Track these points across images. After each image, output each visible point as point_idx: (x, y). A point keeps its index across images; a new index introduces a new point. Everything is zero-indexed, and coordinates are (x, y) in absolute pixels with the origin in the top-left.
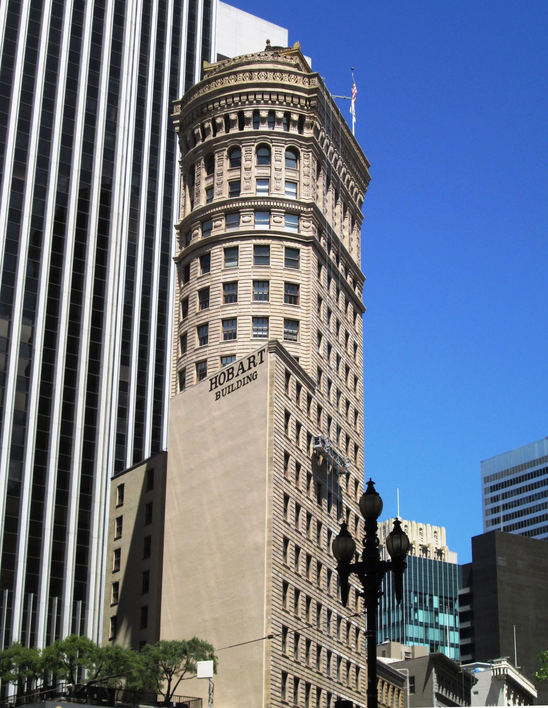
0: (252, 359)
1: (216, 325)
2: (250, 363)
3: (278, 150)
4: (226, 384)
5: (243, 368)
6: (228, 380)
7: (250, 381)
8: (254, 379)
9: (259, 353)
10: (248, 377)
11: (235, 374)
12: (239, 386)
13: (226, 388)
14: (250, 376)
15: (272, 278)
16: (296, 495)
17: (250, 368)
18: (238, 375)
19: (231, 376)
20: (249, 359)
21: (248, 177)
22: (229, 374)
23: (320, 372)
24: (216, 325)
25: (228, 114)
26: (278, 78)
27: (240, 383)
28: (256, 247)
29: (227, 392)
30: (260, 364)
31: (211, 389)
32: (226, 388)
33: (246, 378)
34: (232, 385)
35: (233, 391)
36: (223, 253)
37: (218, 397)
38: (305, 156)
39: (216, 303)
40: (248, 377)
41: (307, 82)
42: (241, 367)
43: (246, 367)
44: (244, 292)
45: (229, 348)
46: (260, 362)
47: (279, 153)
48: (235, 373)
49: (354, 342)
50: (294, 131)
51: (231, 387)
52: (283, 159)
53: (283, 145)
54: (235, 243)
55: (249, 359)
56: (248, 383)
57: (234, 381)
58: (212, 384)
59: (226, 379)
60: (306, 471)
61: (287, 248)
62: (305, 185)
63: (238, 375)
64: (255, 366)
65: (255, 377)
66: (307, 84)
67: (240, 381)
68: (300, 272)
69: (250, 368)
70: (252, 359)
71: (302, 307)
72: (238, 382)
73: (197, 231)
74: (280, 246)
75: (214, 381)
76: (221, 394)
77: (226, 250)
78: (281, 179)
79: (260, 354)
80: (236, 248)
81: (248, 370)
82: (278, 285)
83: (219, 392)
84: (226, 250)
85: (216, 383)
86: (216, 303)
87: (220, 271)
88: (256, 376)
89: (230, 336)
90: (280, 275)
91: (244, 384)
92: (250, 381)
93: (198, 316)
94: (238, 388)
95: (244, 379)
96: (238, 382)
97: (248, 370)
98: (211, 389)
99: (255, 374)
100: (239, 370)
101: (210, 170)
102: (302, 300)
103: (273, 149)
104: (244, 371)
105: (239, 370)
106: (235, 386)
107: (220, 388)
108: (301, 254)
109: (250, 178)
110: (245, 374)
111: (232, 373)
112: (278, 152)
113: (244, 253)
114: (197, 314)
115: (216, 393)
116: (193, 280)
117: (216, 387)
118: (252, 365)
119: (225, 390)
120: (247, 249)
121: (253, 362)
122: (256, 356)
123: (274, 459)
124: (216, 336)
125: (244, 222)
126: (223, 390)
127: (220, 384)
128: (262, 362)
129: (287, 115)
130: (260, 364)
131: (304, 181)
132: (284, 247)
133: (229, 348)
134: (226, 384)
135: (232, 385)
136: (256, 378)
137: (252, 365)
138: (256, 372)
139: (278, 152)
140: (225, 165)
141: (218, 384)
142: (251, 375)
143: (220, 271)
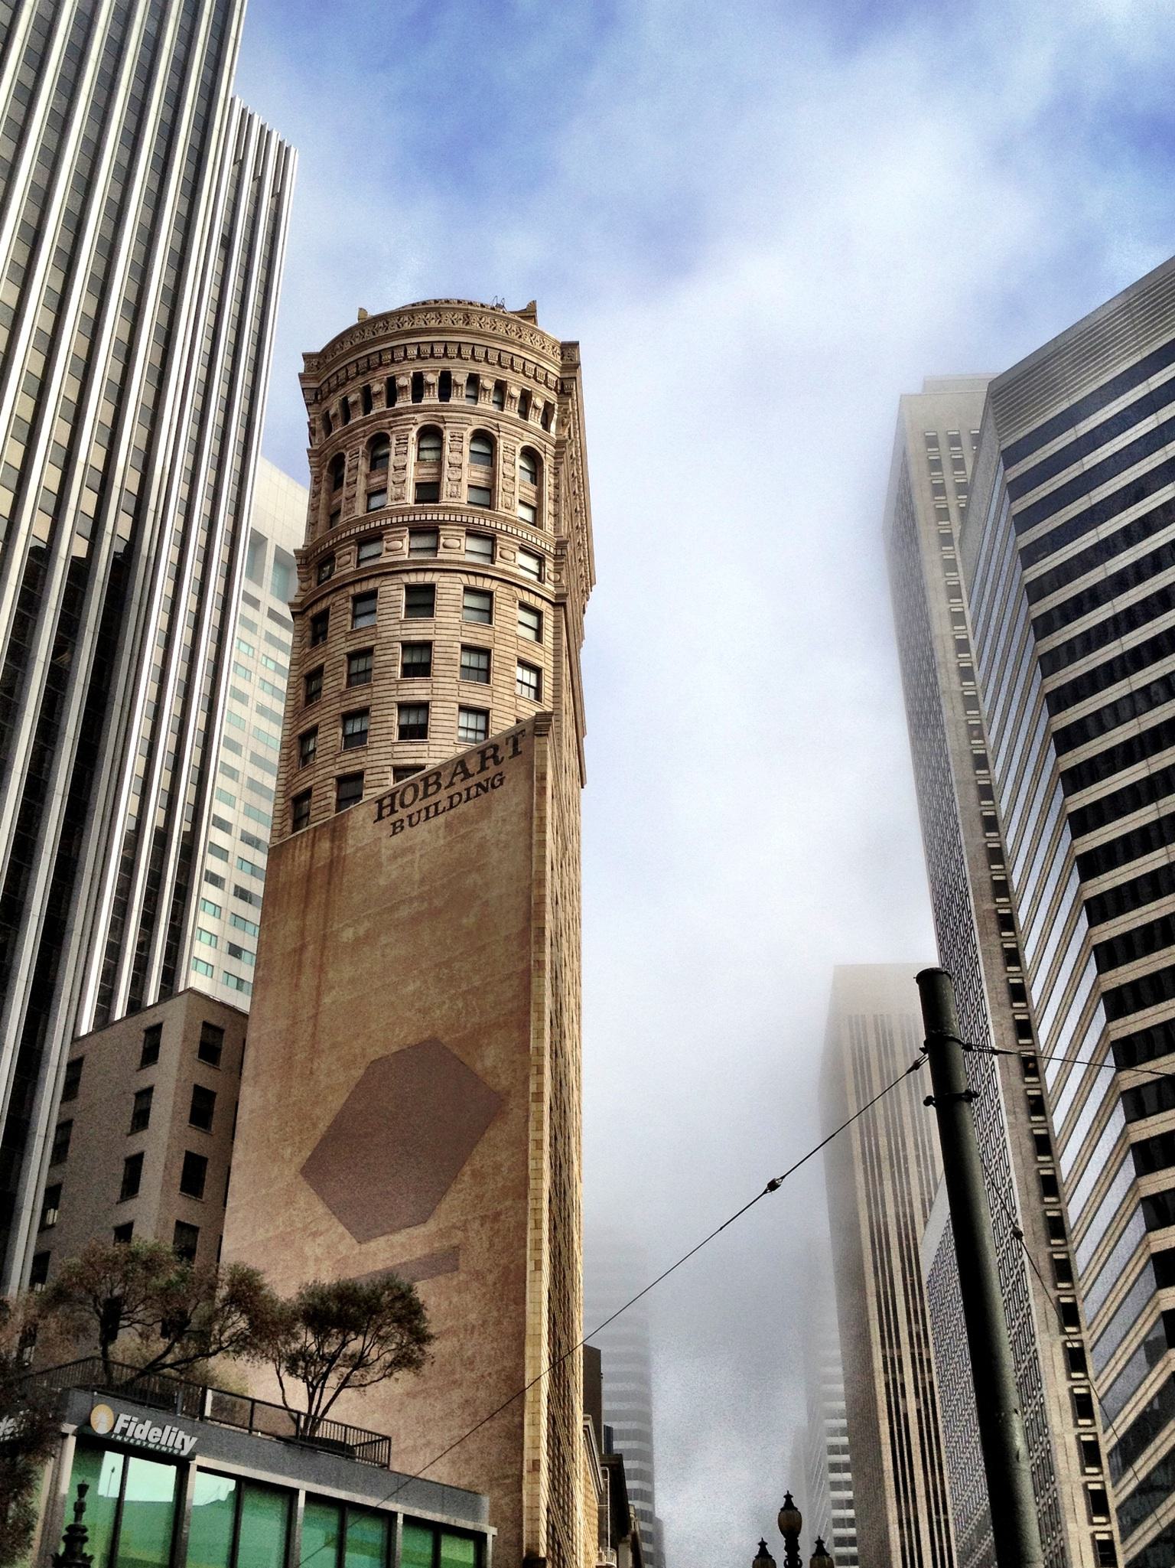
0: (490, 752)
1: (386, 712)
2: (484, 759)
4: (420, 805)
5: (465, 771)
6: (426, 795)
8: (493, 787)
13: (419, 812)
14: (485, 784)
15: (496, 646)
17: (483, 768)
18: (451, 784)
19: (431, 790)
21: (456, 477)
22: (427, 786)
24: (386, 712)
25: (421, 373)
27: (456, 799)
29: (422, 819)
30: (510, 758)
31: (380, 817)
32: (419, 812)
34: (436, 804)
35: (437, 814)
36: (403, 592)
37: (397, 828)
39: (387, 675)
40: (479, 785)
42: (459, 770)
44: (443, 661)
45: (411, 753)
48: (444, 782)
50: (535, 421)
51: (432, 809)
54: (428, 578)
56: (478, 795)
57: (443, 795)
58: (381, 809)
59: (421, 794)
63: (451, 784)
65: (497, 783)
67: (460, 794)
68: (542, 649)
69: (483, 768)
72: (451, 797)
73: (348, 557)
74: (511, 598)
75: (387, 802)
76: (406, 823)
77: (411, 589)
80: (430, 589)
81: (478, 772)
82: (507, 661)
83: (402, 821)
84: (411, 589)
85: (392, 805)
86: (387, 675)
87: (396, 621)
88: (501, 781)
89: (415, 732)
91: (468, 799)
92: (485, 790)
93: (345, 697)
94: (451, 807)
95: (468, 790)
97: (478, 772)
98: (380, 817)
99: (499, 777)
100: (455, 774)
101: (378, 463)
103: (501, 443)
104: (467, 775)
105: (455, 774)
106: (446, 804)
107: (402, 813)
109: (460, 480)
110: (471, 782)
113: (444, 597)
114: (342, 694)
115: (394, 824)
116: (336, 637)
117: (393, 811)
118: (490, 763)
119: (416, 815)
120: (451, 591)
121: (494, 756)
124: (385, 731)
125: (445, 547)
126: (410, 817)
127: (403, 805)
128: (516, 753)
130: (510, 758)
133: (411, 753)
134: (420, 805)
135: (436, 804)
136: (501, 784)
137: (490, 763)
138: (501, 774)
140: (409, 453)
141: (397, 807)
142: (487, 780)
143: (396, 621)
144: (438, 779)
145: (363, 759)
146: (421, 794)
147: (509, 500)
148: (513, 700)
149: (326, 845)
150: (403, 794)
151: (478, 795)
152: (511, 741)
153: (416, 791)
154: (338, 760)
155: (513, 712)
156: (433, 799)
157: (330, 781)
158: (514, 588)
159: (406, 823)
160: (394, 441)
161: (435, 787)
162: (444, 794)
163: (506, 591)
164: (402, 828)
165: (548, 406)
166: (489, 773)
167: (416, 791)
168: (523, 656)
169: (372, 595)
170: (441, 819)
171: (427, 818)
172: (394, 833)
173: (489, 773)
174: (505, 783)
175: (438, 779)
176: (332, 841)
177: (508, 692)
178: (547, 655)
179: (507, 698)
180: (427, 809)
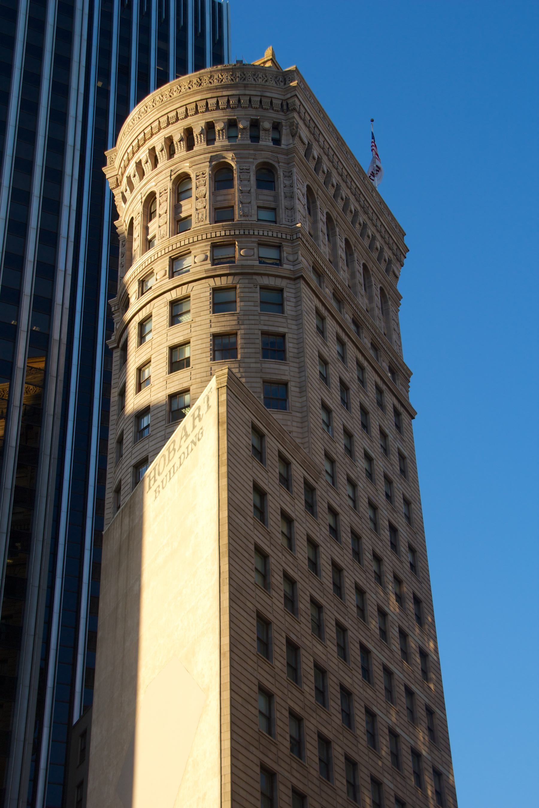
3: (244, 168)
5: (186, 433)
6: (169, 461)
7: (195, 444)
8: (199, 440)
11: (177, 449)
14: (195, 440)
16: (287, 624)
28: (215, 290)
33: (191, 444)
34: (174, 466)
38: (285, 174)
40: (193, 442)
41: (282, 81)
42: (184, 434)
47: (246, 171)
48: (177, 447)
49: (399, 449)
50: (266, 141)
53: (251, 160)
60: (308, 594)
61: (263, 288)
62: (287, 209)
66: (282, 84)
69: (194, 427)
71: (292, 364)
74: (252, 285)
78: (250, 203)
85: (154, 477)
88: (202, 433)
90: (253, 322)
92: (195, 444)
94: (181, 465)
96: (180, 458)
102: (291, 354)
106: (178, 464)
108: (286, 294)
110: (190, 439)
111: (174, 449)
112: (243, 171)
115: (155, 491)
117: (155, 481)
129: (255, 125)
130: (206, 413)
131: (286, 204)
132: (258, 287)
135: (174, 466)
138: (201, 429)
139: (243, 171)
144: (174, 446)
145: (147, 446)
146: (167, 464)
147: (246, 210)
148: (259, 365)
149: (126, 521)
150: (159, 466)
151: (192, 450)
152: (206, 399)
153: (165, 460)
154: (134, 452)
155: (259, 375)
156: (171, 464)
157: (130, 469)
158: (255, 277)
159: (161, 487)
160: (157, 196)
161: (173, 452)
162: (178, 455)
163: (247, 281)
164: (159, 492)
165: (276, 127)
167: (165, 460)
168: (265, 328)
169: (149, 317)
170: (175, 478)
171: (170, 479)
172: (156, 497)
173: (197, 430)
174: (204, 433)
175: (174, 446)
176: (130, 517)
177: (253, 360)
178: (289, 321)
179: (252, 365)
180: (170, 471)
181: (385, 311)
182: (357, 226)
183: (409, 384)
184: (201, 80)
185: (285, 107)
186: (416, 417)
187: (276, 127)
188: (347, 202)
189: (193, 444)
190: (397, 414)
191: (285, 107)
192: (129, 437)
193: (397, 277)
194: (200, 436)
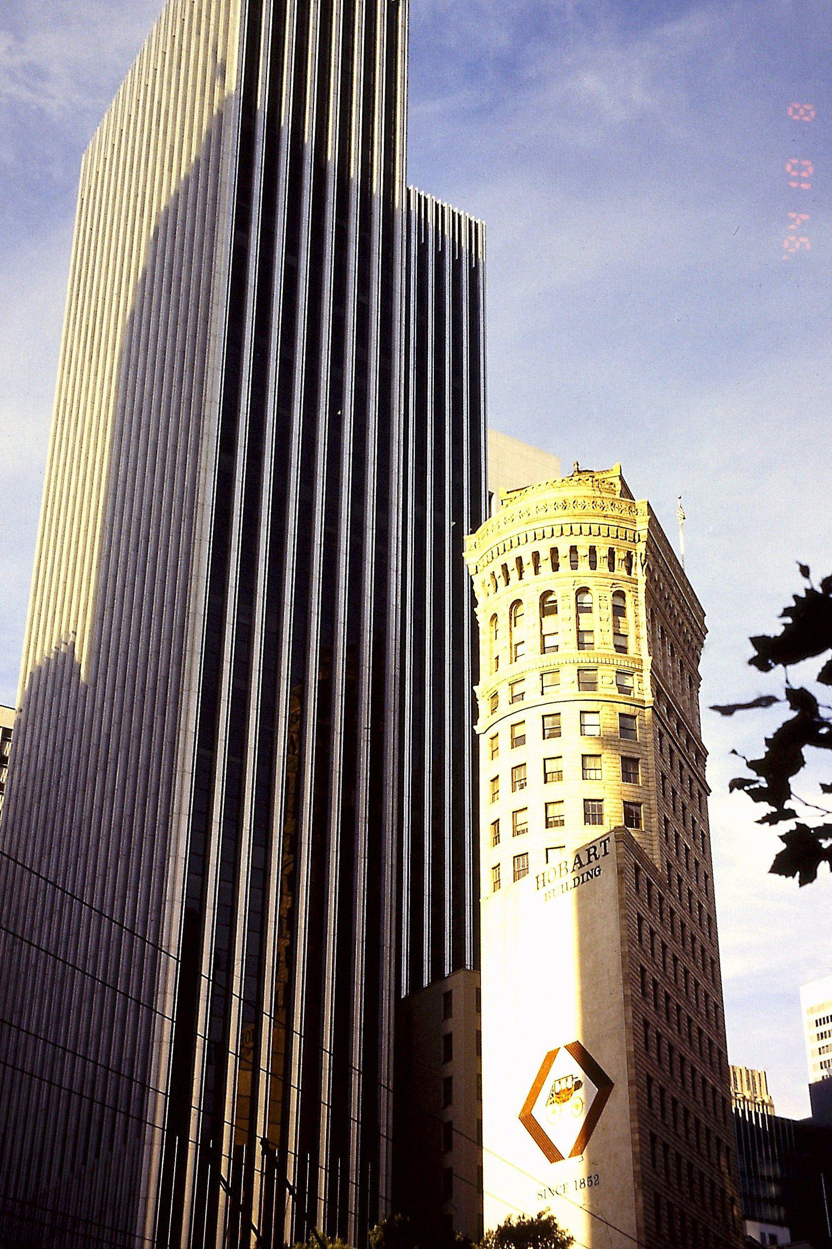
0: (592, 851)
2: (589, 855)
5: (580, 862)
9: (601, 843)
10: (588, 873)
12: (576, 885)
14: (591, 872)
20: (588, 850)
23: (669, 866)
26: (598, 507)
27: (577, 880)
42: (577, 861)
43: (584, 861)
46: (603, 854)
50: (620, 571)
52: (610, 607)
55: (588, 850)
64: (596, 859)
65: (597, 873)
69: (590, 862)
70: (592, 851)
74: (612, 713)
79: (603, 844)
81: (587, 864)
88: (599, 871)
92: (592, 877)
95: (583, 875)
96: (574, 879)
97: (587, 864)
99: (598, 869)
100: (575, 864)
104: (582, 866)
118: (592, 857)
121: (594, 854)
122: (598, 847)
123: (631, 976)
136: (600, 873)
137: (592, 857)
138: (599, 867)
151: (588, 880)
166: (593, 865)
168: (624, 754)
173: (593, 865)
181: (691, 699)
182: (678, 626)
183: (706, 763)
184: (565, 503)
185: (637, 538)
186: (711, 794)
187: (629, 557)
188: (672, 609)
189: (589, 876)
190: (700, 795)
191: (637, 538)
192: (506, 829)
193: (699, 661)
194: (597, 873)
